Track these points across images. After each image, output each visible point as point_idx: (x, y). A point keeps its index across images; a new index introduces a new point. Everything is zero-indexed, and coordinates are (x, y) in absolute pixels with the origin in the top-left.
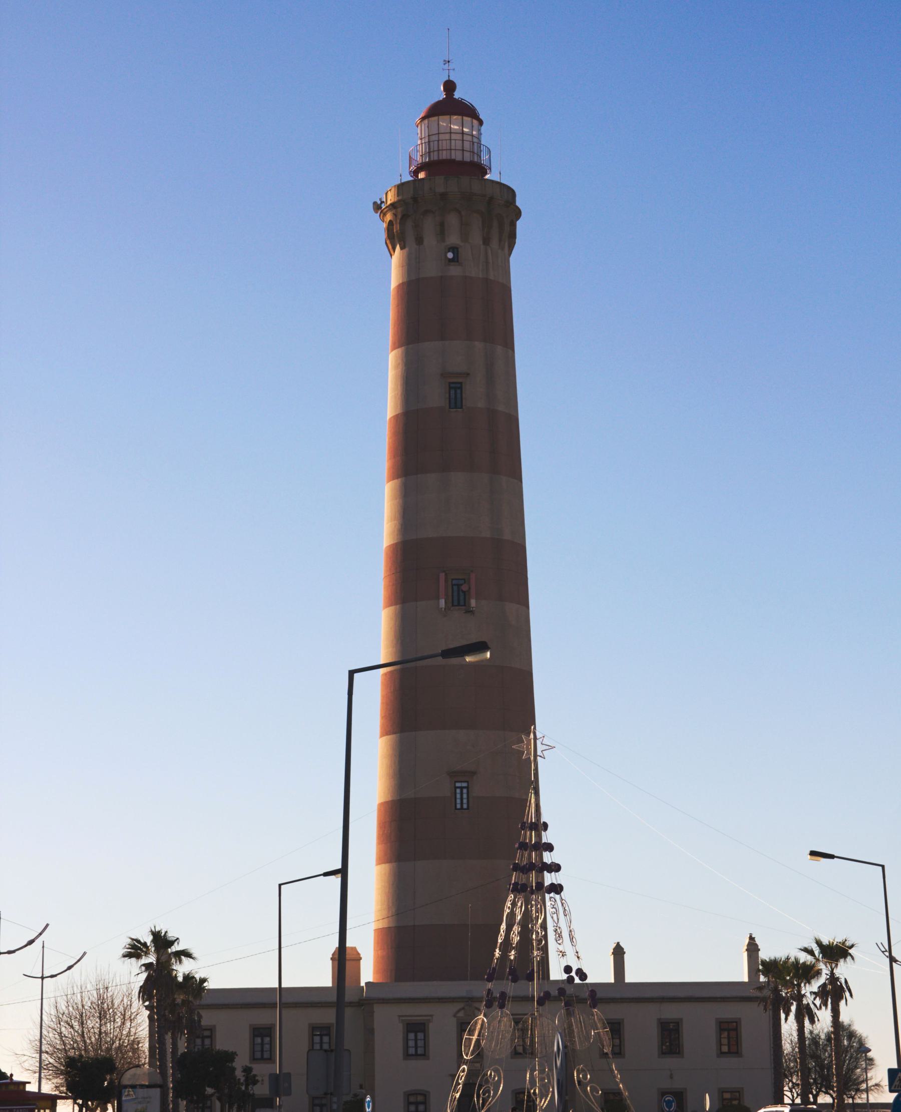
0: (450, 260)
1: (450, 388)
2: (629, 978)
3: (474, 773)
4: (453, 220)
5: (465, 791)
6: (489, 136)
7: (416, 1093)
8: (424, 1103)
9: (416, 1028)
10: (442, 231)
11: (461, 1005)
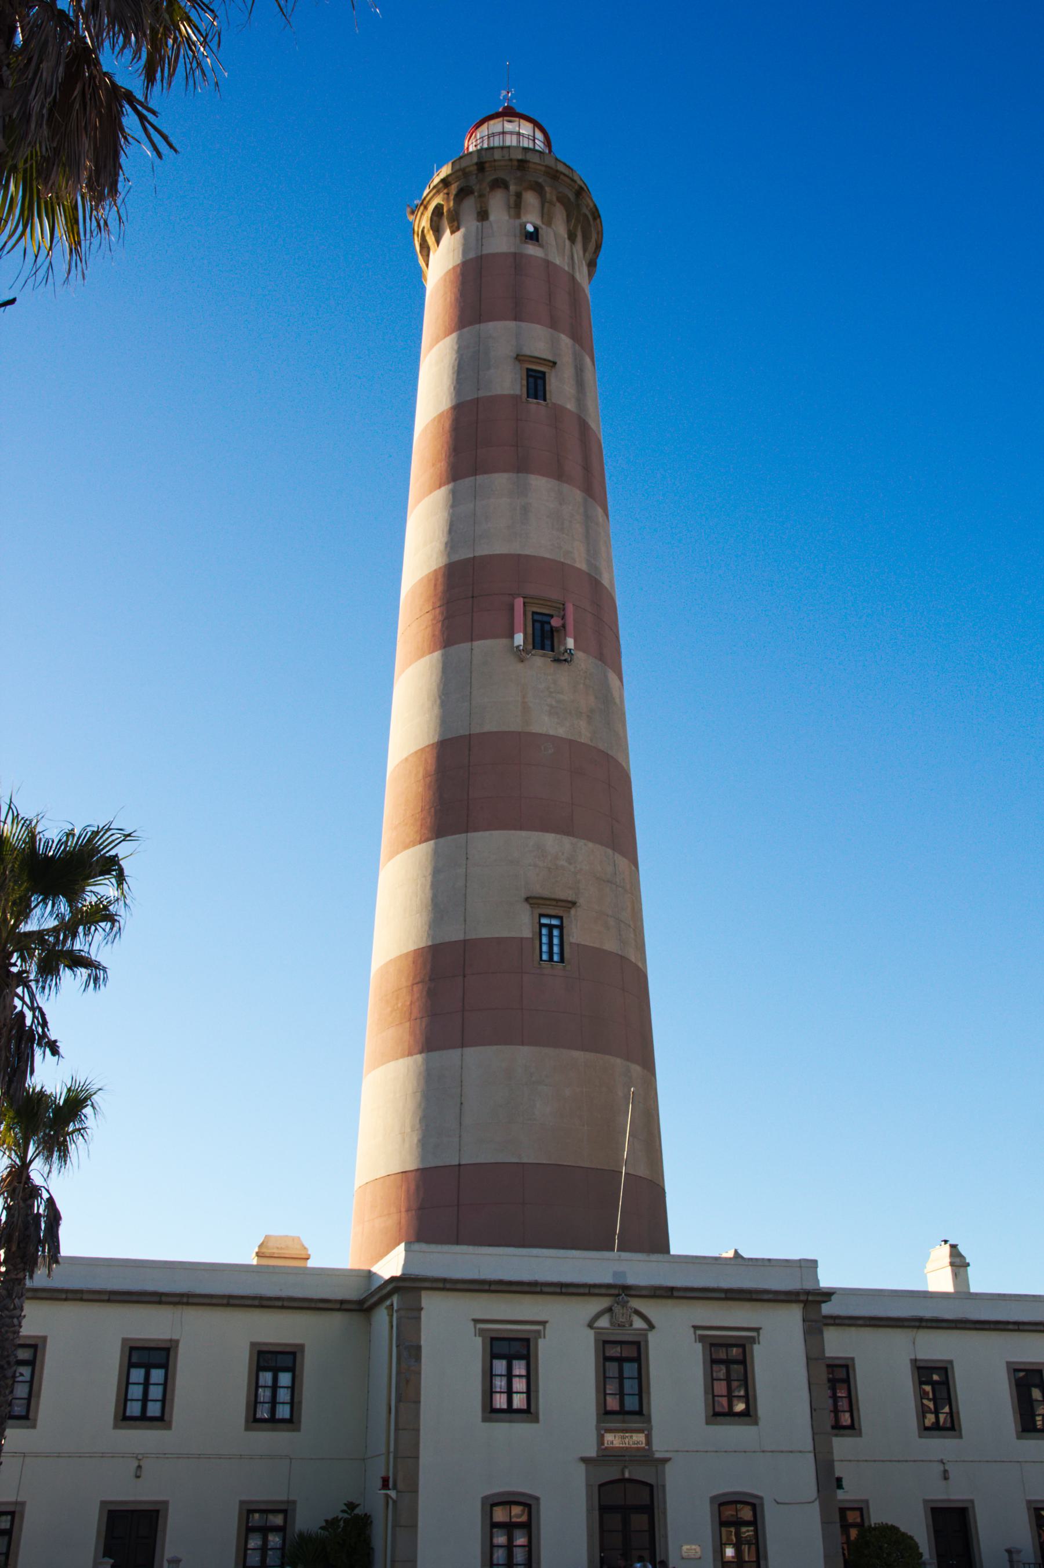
1: (528, 376)
3: (574, 904)
4: (531, 199)
5: (556, 932)
7: (507, 1501)
8: (527, 1527)
9: (511, 1349)
10: (517, 207)
11: (604, 1303)
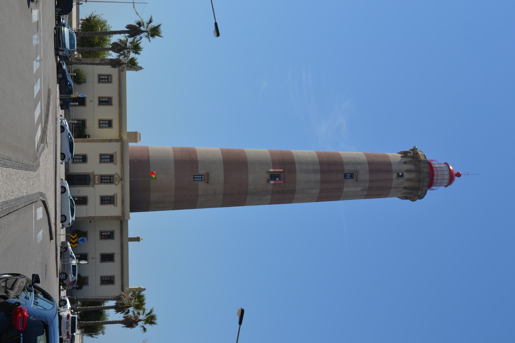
0: (398, 174)
2: (130, 243)
3: (208, 183)
4: (413, 175)
6: (442, 189)
11: (120, 176)
